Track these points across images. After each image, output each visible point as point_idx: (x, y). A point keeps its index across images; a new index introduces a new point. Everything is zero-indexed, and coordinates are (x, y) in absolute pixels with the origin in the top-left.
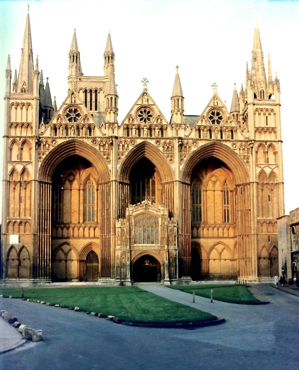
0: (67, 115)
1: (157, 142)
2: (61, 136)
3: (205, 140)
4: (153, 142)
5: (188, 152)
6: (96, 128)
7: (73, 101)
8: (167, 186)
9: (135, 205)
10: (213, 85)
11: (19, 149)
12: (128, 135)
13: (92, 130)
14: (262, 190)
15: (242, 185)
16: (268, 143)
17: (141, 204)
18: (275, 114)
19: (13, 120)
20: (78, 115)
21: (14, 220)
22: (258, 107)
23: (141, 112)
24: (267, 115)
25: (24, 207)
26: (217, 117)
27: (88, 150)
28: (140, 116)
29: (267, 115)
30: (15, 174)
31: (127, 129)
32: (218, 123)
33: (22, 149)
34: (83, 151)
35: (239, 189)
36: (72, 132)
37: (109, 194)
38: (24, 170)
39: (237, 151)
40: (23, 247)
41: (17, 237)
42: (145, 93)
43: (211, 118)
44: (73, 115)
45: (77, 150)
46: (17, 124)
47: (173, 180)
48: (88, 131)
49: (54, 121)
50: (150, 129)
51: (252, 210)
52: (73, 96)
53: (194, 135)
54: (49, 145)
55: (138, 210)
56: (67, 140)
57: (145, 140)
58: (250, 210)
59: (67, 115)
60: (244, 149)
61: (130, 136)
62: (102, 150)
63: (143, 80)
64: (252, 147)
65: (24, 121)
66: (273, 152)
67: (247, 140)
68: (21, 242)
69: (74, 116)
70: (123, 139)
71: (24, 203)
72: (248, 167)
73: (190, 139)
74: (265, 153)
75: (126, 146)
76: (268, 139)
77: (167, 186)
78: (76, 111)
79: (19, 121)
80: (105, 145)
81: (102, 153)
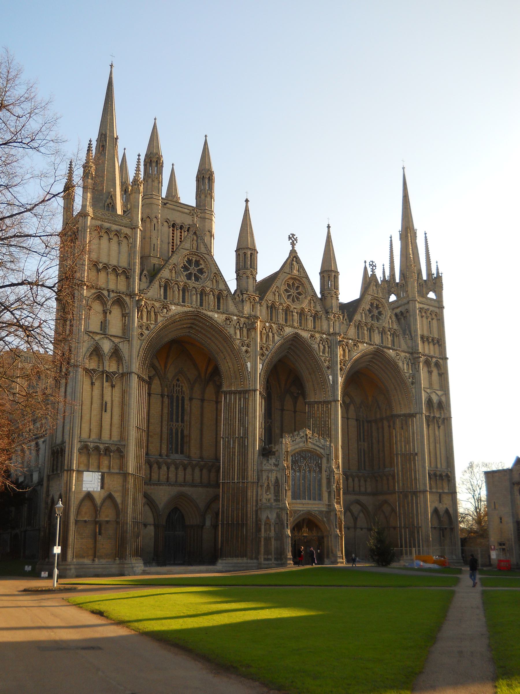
0: (185, 268)
1: (312, 336)
2: (176, 301)
3: (366, 343)
4: (305, 335)
5: (347, 358)
6: (229, 299)
7: (195, 246)
8: (318, 407)
9: (291, 435)
10: (371, 263)
11: (105, 313)
12: (271, 320)
13: (221, 301)
14: (428, 426)
15: (405, 415)
16: (434, 360)
17: (299, 434)
18: (438, 320)
19: (94, 256)
20: (201, 271)
21: (91, 445)
22: (422, 306)
23: (288, 285)
24: (429, 319)
25: (109, 420)
26: (377, 311)
27: (214, 333)
28: (286, 290)
29: (429, 319)
30: (95, 358)
31: (272, 308)
32: (378, 319)
33: (110, 313)
34: (204, 332)
35: (398, 422)
36: (194, 297)
37: (244, 412)
38: (116, 353)
39: (400, 364)
40: (110, 497)
41: (97, 476)
42: (295, 257)
43: (370, 311)
44: (193, 269)
45: (194, 329)
46: (106, 267)
47: (331, 399)
48: (216, 300)
49: (165, 274)
50: (302, 314)
51: (420, 455)
52: (195, 237)
53: (352, 332)
54: (156, 315)
55: (297, 444)
56: (186, 309)
57: (296, 331)
58: (416, 454)
59: (185, 268)
60: (408, 364)
61: (274, 319)
62: (238, 337)
63: (291, 236)
64: (419, 363)
65: (114, 262)
66: (437, 372)
67: (410, 350)
68: (106, 486)
69: (194, 272)
70: (267, 324)
71: (110, 413)
72: (414, 390)
73: (350, 339)
74: (430, 372)
75: (271, 334)
76: (432, 353)
77: (318, 407)
78: (197, 263)
79: (104, 259)
80: (243, 328)
81: (238, 342)
